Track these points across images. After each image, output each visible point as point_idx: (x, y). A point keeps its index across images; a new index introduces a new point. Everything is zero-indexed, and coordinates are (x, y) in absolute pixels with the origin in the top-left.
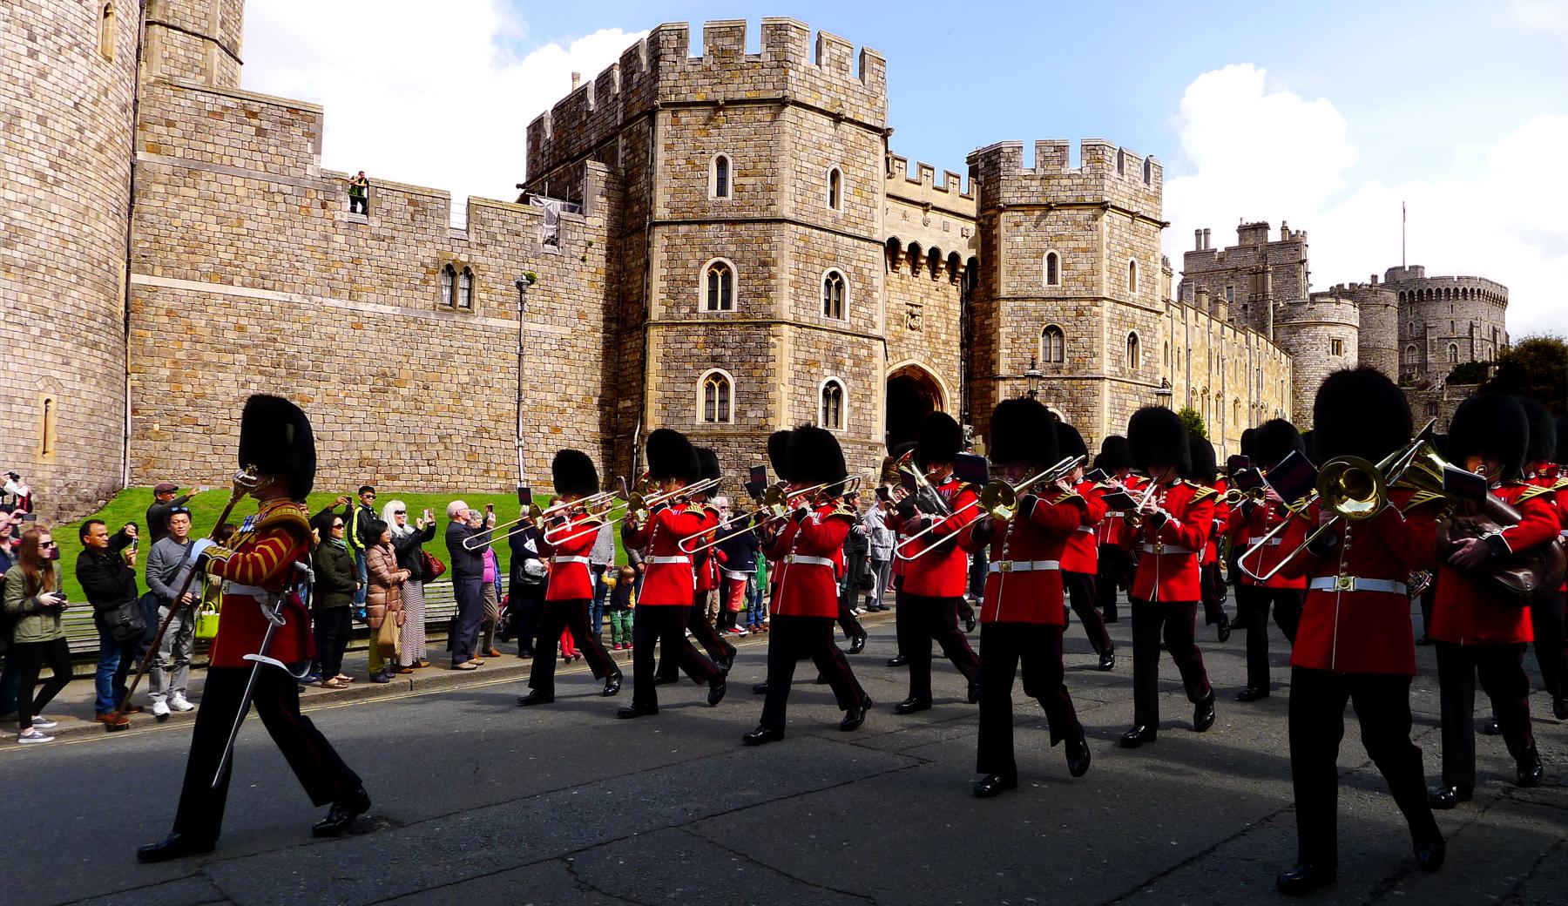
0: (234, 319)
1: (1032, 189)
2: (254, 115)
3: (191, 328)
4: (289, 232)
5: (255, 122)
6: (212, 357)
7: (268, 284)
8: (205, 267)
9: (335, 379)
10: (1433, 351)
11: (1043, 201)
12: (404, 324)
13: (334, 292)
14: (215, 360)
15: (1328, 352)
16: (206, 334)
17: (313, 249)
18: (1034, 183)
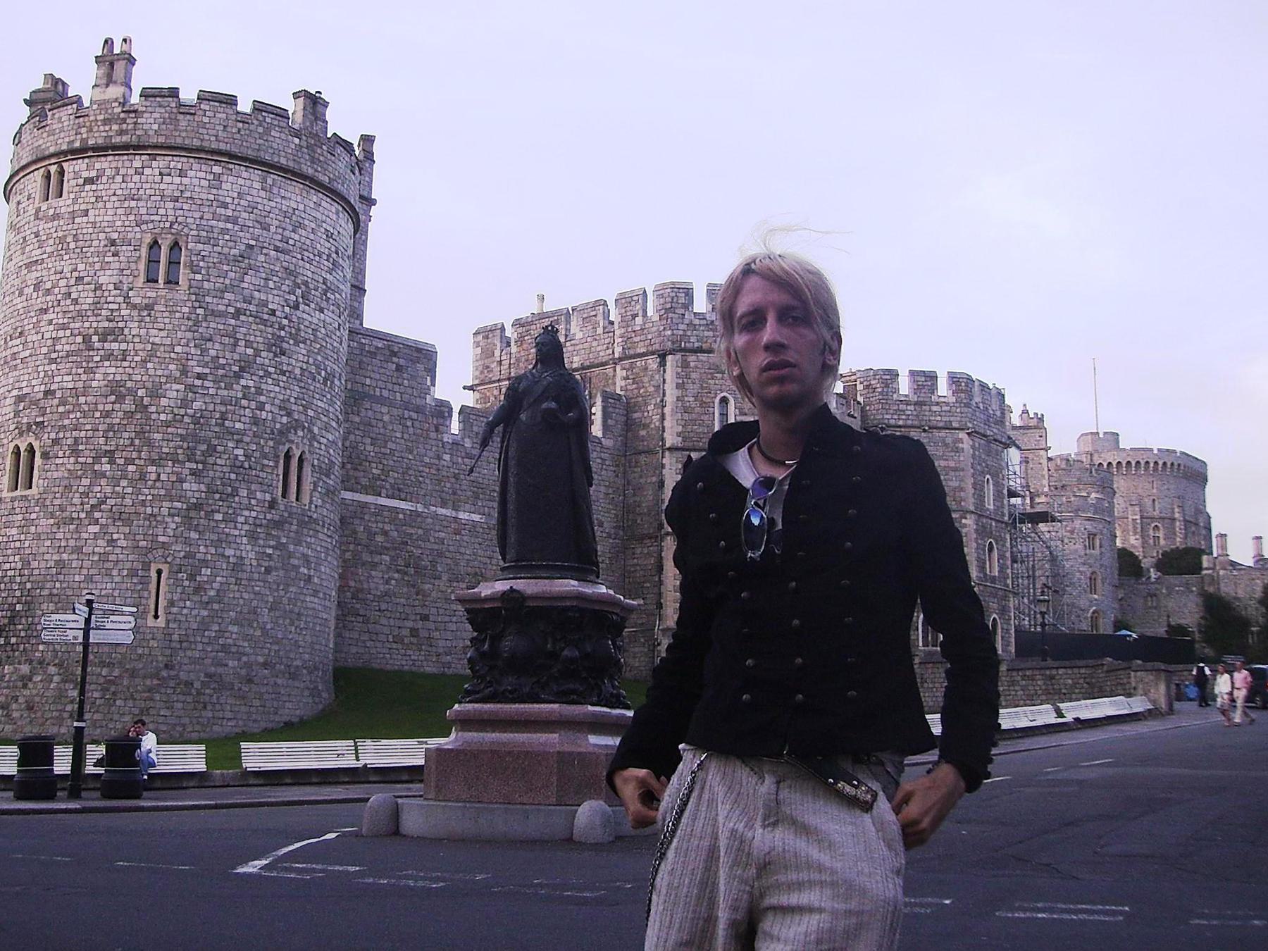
0: (380, 525)
1: (909, 413)
2: (394, 354)
3: (355, 532)
4: (415, 452)
5: (395, 360)
6: (366, 557)
7: (403, 496)
8: (364, 481)
9: (445, 577)
10: (1135, 533)
11: (916, 423)
12: (487, 531)
13: (444, 504)
14: (370, 560)
15: (1085, 546)
16: (362, 536)
17: (430, 466)
18: (909, 408)
